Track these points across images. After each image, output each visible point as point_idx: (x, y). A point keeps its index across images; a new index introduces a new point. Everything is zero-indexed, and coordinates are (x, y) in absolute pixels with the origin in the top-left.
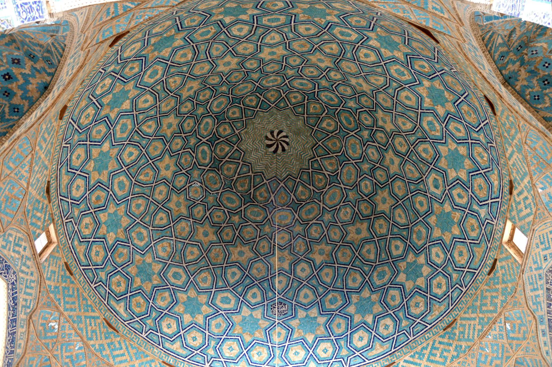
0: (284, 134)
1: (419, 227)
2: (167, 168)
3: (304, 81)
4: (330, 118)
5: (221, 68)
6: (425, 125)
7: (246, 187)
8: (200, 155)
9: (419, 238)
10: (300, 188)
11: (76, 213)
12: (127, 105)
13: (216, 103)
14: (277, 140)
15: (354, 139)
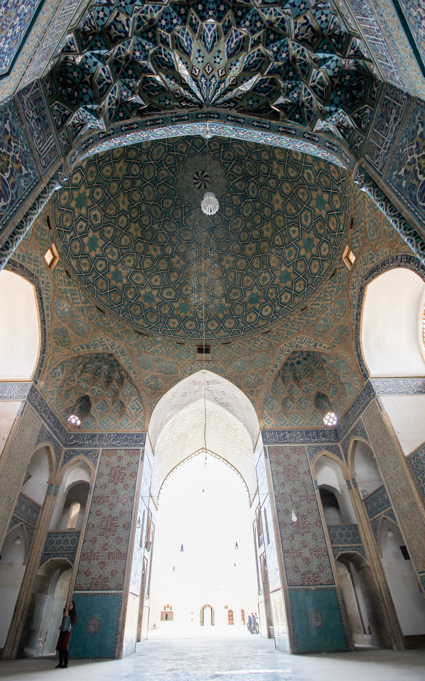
0: (197, 186)
1: (93, 178)
2: (277, 201)
3: (185, 238)
4: (167, 209)
5: (232, 259)
6: (115, 250)
7: (226, 153)
8: (256, 191)
9: (91, 171)
10: (184, 150)
11: (332, 239)
12: (284, 268)
13: (239, 225)
14: (202, 180)
15: (150, 200)
